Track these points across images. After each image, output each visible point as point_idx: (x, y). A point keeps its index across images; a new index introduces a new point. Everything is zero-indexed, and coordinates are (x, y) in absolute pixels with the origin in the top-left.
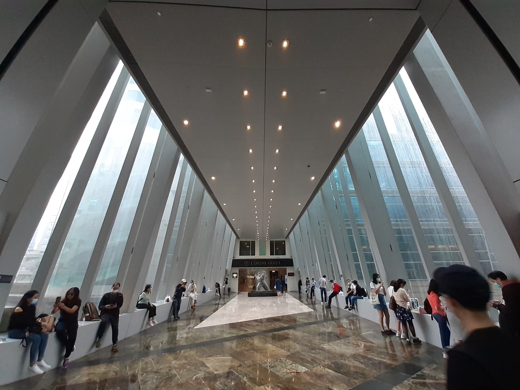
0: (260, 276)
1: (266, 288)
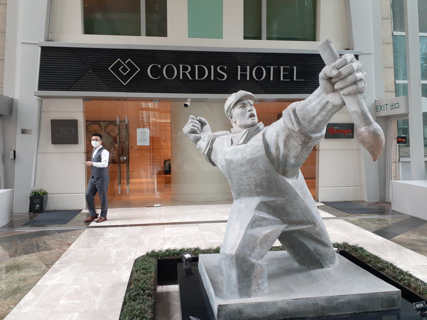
1: (311, 245)
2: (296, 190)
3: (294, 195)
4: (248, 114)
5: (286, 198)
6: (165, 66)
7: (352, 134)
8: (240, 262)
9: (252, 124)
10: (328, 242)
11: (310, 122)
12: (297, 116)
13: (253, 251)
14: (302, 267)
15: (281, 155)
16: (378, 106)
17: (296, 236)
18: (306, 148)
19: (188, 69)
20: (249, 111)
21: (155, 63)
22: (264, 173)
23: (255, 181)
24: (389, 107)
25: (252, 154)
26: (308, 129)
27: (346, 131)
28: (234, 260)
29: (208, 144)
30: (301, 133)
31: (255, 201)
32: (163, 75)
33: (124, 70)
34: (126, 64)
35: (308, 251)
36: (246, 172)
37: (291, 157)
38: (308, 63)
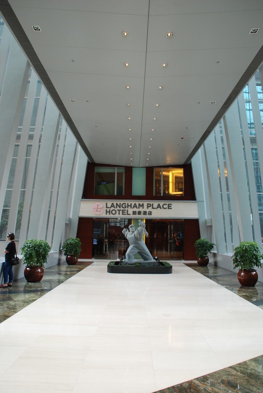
0: (133, 232)
1: (145, 255)
31: (133, 245)
35: (144, 256)
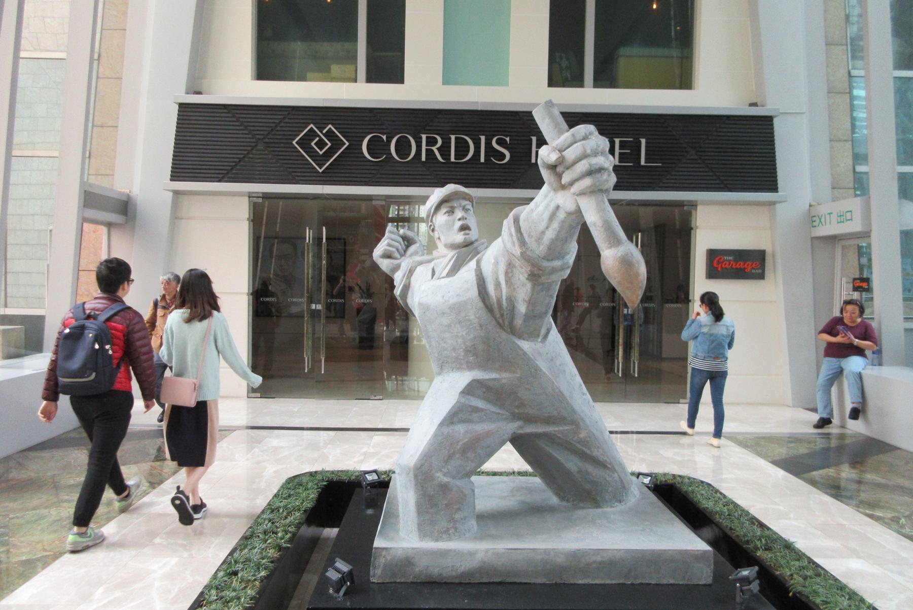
1: (572, 464)
2: (537, 362)
3: (533, 371)
4: (458, 224)
5: (518, 375)
6: (393, 137)
7: (760, 271)
8: (421, 479)
9: (464, 242)
10: (608, 460)
11: (539, 240)
12: (520, 229)
13: (446, 462)
14: (565, 504)
15: (504, 298)
16: (815, 216)
17: (542, 444)
18: (541, 286)
19: (436, 142)
20: (459, 219)
21: (375, 131)
22: (478, 330)
23: (464, 343)
24: (834, 218)
25: (458, 295)
26: (537, 252)
27: (748, 265)
28: (411, 475)
29: (404, 277)
30: (525, 259)
31: (464, 378)
32: (391, 154)
33: (321, 144)
34: (325, 135)
35: (567, 473)
36: (449, 326)
37: (520, 301)
38: (670, 131)
